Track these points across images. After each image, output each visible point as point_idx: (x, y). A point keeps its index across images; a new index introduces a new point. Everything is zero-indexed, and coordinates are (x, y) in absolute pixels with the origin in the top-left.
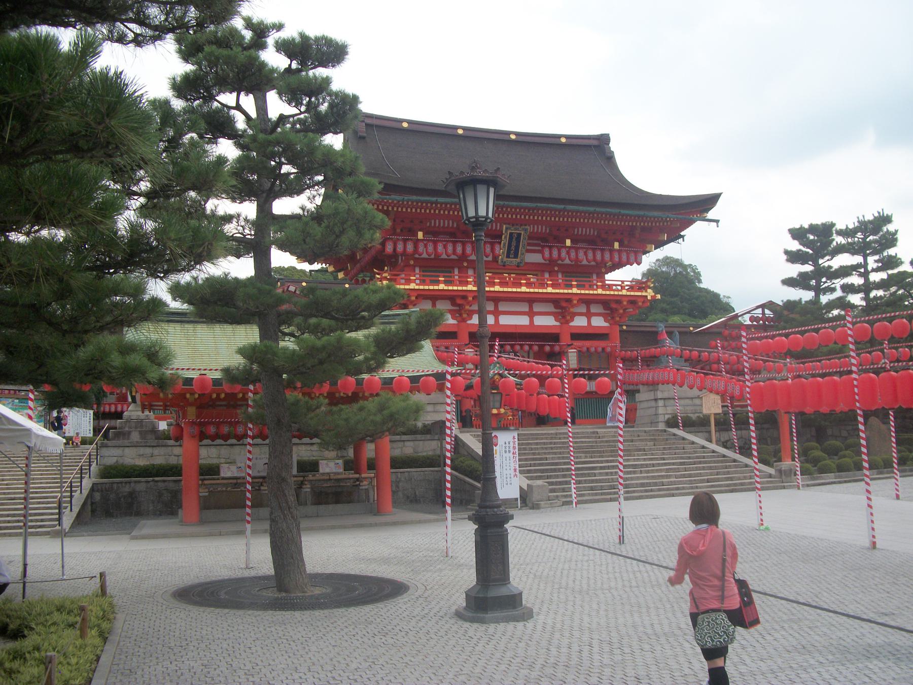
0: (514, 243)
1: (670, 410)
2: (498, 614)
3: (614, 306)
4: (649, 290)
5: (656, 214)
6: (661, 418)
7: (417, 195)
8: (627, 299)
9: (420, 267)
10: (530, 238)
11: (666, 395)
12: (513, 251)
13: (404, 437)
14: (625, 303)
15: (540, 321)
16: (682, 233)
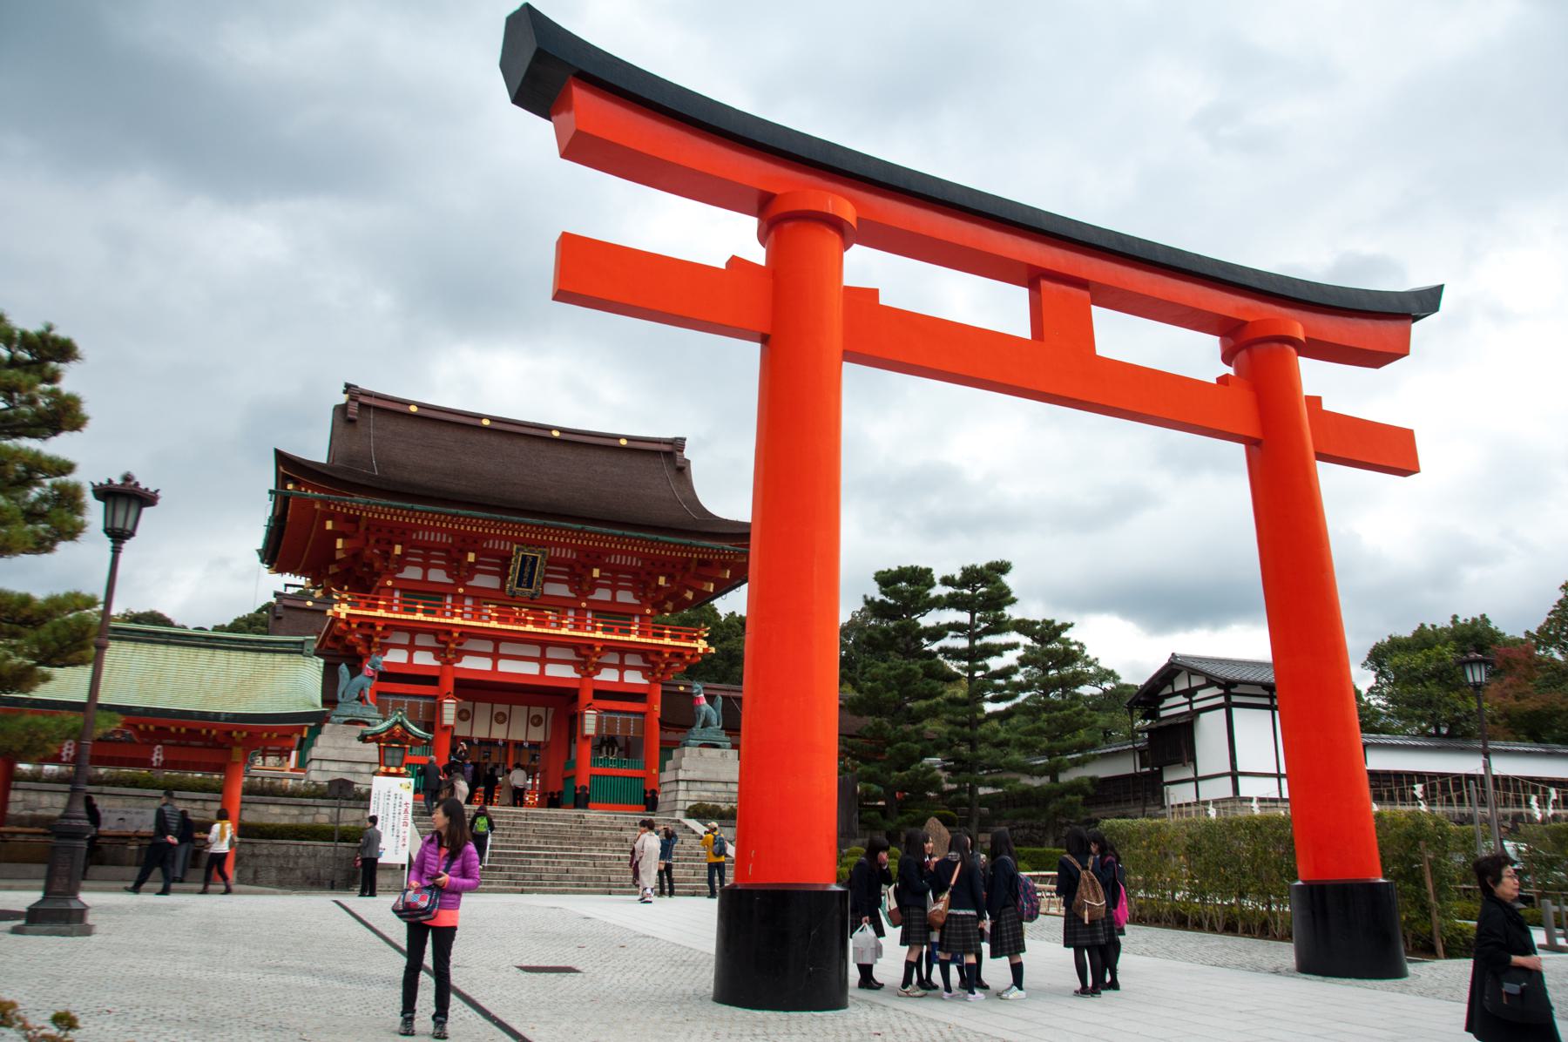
0: (528, 569)
1: (693, 795)
2: (46, 928)
3: (652, 658)
5: (707, 543)
6: (680, 805)
9: (401, 590)
10: (549, 563)
11: (690, 775)
12: (526, 579)
13: (319, 801)
15: (553, 671)
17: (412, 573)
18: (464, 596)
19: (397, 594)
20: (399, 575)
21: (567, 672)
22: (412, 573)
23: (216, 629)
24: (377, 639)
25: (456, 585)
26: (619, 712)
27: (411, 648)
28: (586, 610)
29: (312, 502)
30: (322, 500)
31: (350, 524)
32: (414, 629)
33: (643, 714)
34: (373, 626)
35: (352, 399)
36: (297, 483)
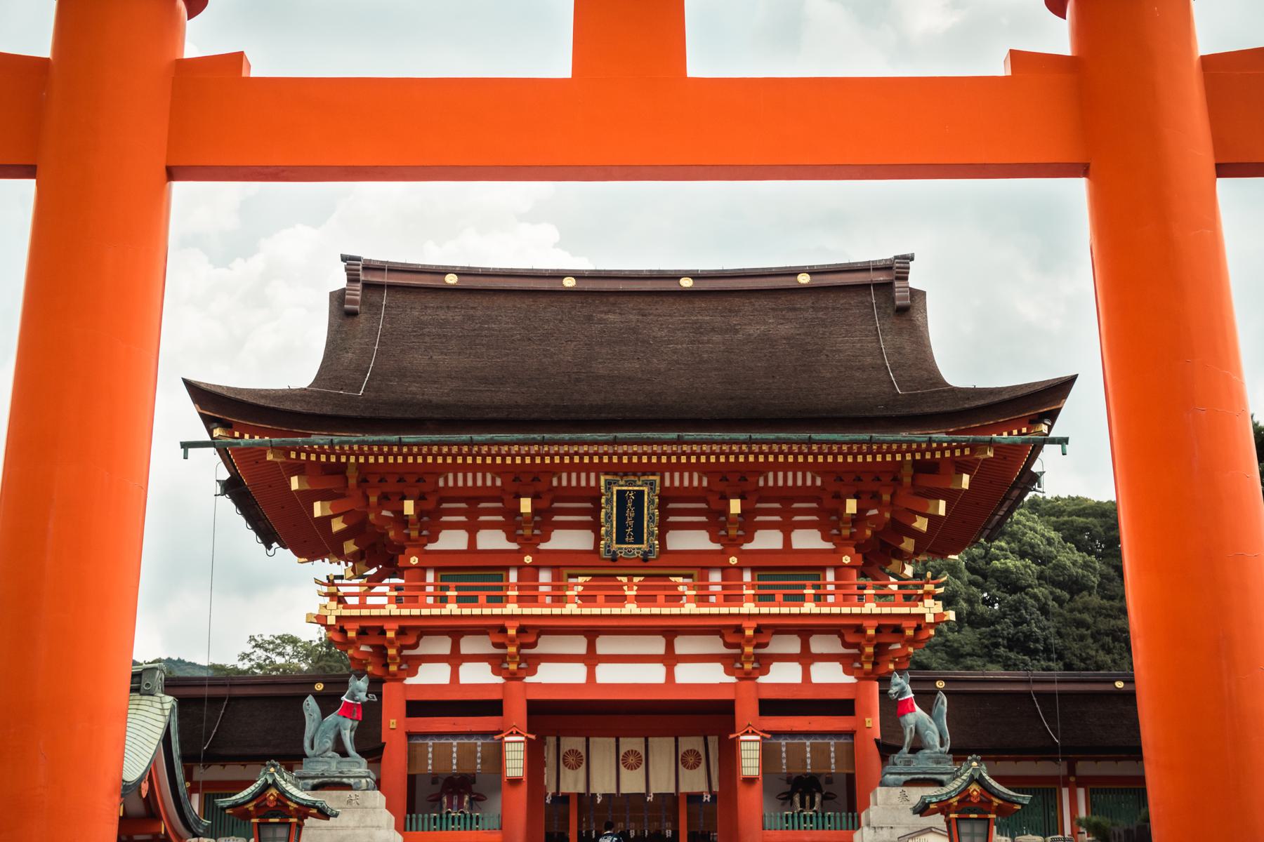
0: (630, 513)
3: (851, 638)
4: (929, 602)
5: (903, 435)
7: (364, 432)
8: (875, 623)
9: (437, 569)
14: (871, 632)
15: (687, 674)
16: (1035, 468)
17: (452, 541)
18: (536, 568)
19: (430, 577)
20: (431, 547)
21: (713, 674)
22: (452, 541)
23: (154, 662)
25: (521, 553)
26: (808, 734)
27: (455, 659)
29: (260, 451)
30: (274, 448)
31: (330, 478)
32: (456, 630)
33: (851, 734)
34: (382, 632)
35: (352, 278)
36: (226, 425)
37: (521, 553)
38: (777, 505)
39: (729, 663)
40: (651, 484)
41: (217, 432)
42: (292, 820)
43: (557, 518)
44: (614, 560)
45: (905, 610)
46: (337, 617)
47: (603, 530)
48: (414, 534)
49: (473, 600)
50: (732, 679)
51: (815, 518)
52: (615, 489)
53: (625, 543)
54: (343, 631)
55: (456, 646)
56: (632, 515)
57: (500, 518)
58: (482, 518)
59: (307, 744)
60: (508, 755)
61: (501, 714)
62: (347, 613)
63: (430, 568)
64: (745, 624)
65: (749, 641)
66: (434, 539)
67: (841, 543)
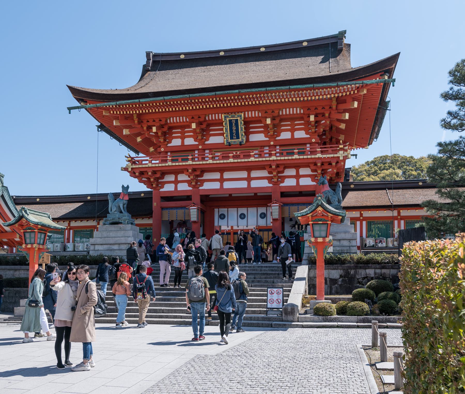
0: (234, 128)
4: (341, 152)
15: (255, 184)
18: (204, 150)
21: (265, 184)
22: (176, 142)
24: (152, 180)
28: (275, 146)
36: (85, 102)
37: (198, 145)
38: (289, 123)
39: (270, 179)
40: (240, 116)
41: (82, 104)
42: (35, 231)
43: (211, 133)
44: (230, 145)
45: (332, 155)
46: (132, 169)
47: (225, 135)
48: (162, 140)
49: (176, 160)
50: (271, 185)
51: (303, 126)
52: (228, 119)
53: (233, 139)
54: (135, 173)
55: (176, 178)
56: (235, 129)
57: (192, 134)
58: (186, 134)
59: (109, 210)
60: (191, 213)
61: (191, 200)
62: (134, 166)
63: (169, 152)
64: (272, 164)
65: (274, 170)
66: (171, 142)
67: (312, 134)
